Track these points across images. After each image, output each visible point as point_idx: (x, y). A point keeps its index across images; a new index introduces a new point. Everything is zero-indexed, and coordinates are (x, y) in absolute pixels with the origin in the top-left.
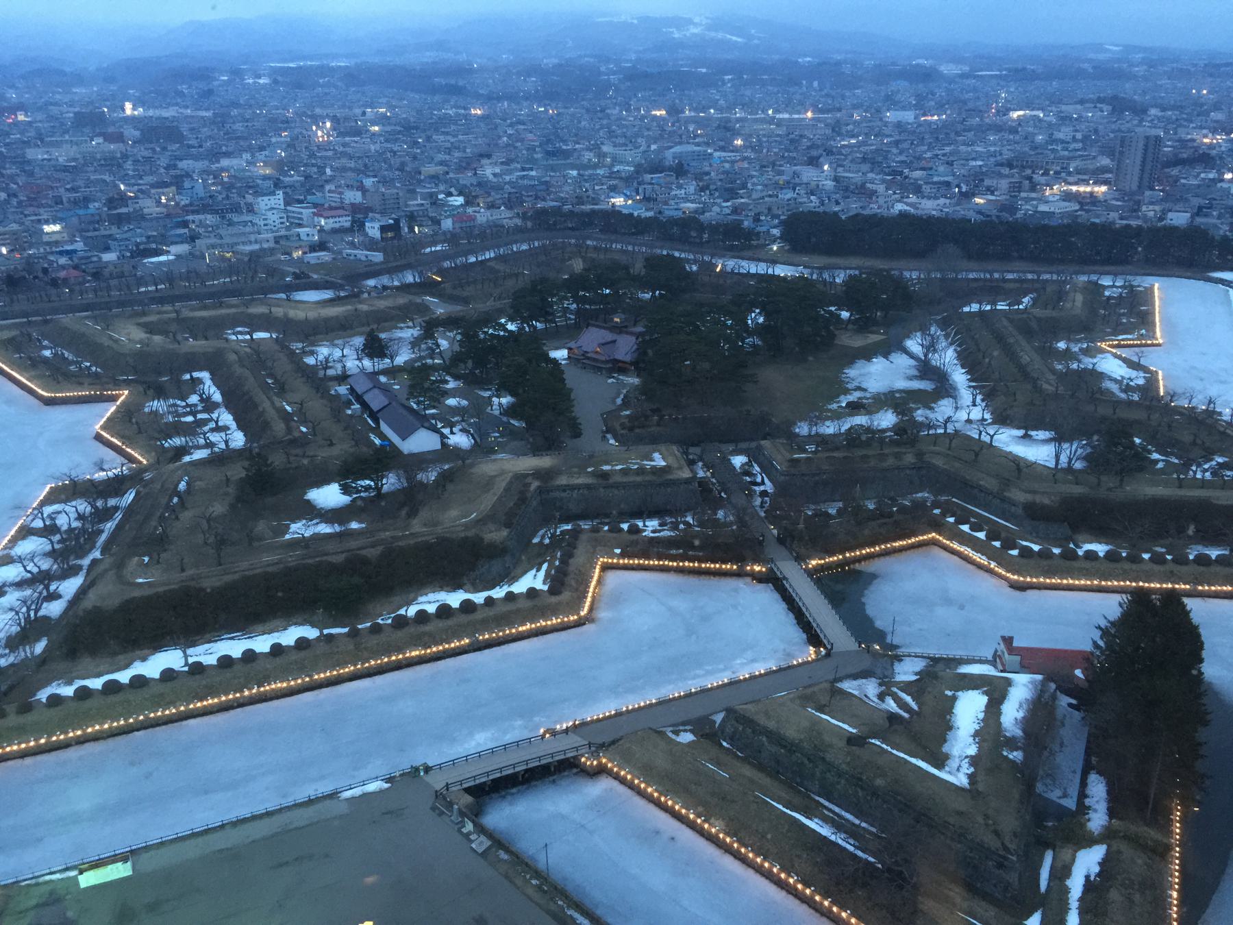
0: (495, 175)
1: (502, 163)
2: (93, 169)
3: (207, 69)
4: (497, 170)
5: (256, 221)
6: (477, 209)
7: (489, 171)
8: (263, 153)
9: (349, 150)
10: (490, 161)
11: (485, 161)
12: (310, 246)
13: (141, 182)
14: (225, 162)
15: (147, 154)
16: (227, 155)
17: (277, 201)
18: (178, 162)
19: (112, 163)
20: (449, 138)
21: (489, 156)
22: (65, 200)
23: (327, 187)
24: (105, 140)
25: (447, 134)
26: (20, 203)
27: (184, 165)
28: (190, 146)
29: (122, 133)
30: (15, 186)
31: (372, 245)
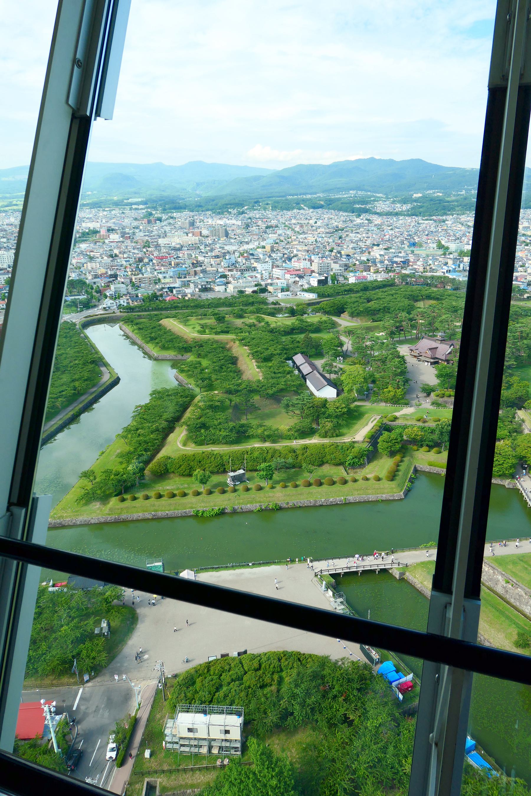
0: (380, 255)
1: (385, 249)
2: (186, 249)
3: (243, 201)
4: (382, 253)
5: (257, 275)
6: (369, 273)
7: (376, 253)
8: (265, 242)
9: (306, 241)
10: (378, 248)
11: (375, 248)
12: (282, 289)
13: (207, 255)
14: (246, 247)
15: (210, 242)
16: (247, 243)
17: (268, 266)
18: (224, 246)
19: (194, 247)
20: (358, 235)
21: (378, 245)
22: (173, 263)
23: (293, 259)
24: (193, 235)
25: (358, 233)
26: (153, 264)
27: (228, 248)
28: (231, 238)
29: (201, 232)
30: (152, 256)
31: (311, 290)
